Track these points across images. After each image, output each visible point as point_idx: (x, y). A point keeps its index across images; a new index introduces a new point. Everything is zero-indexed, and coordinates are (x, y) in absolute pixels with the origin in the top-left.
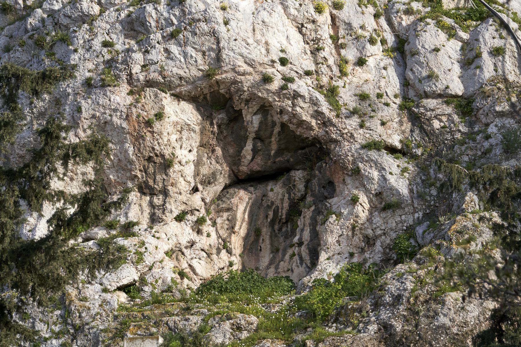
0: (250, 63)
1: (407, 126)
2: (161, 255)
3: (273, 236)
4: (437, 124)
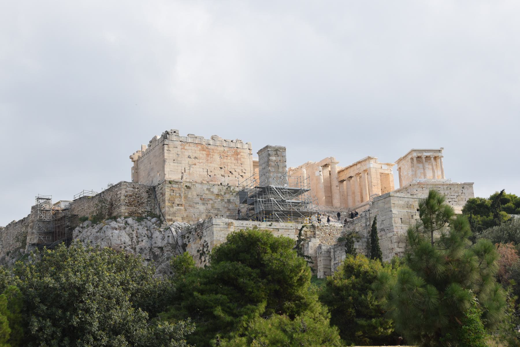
4: (156, 253)
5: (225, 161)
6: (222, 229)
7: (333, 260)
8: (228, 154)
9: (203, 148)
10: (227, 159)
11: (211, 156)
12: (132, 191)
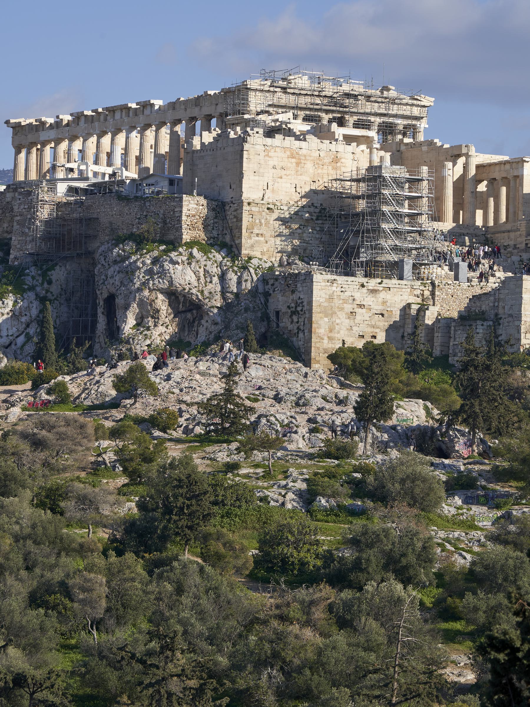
0: (180, 285)
1: (222, 301)
2: (157, 336)
3: (189, 327)
5: (320, 171)
6: (323, 288)
7: (452, 340)
8: (325, 161)
9: (292, 154)
10: (322, 168)
11: (303, 165)
12: (196, 208)
